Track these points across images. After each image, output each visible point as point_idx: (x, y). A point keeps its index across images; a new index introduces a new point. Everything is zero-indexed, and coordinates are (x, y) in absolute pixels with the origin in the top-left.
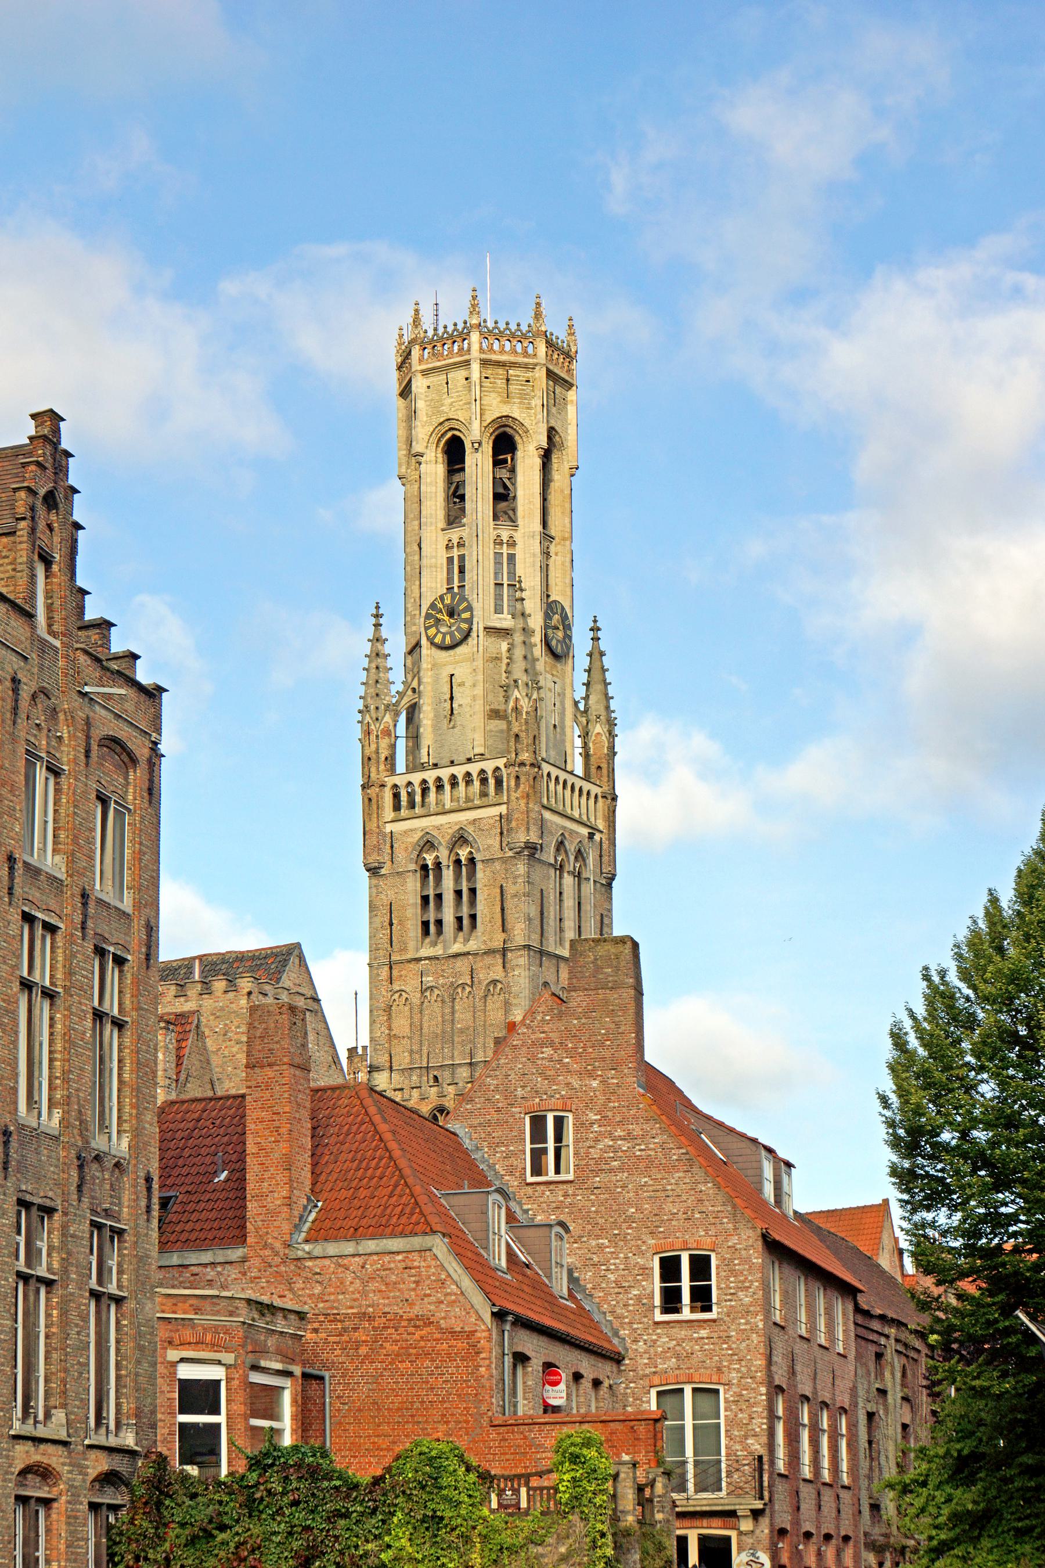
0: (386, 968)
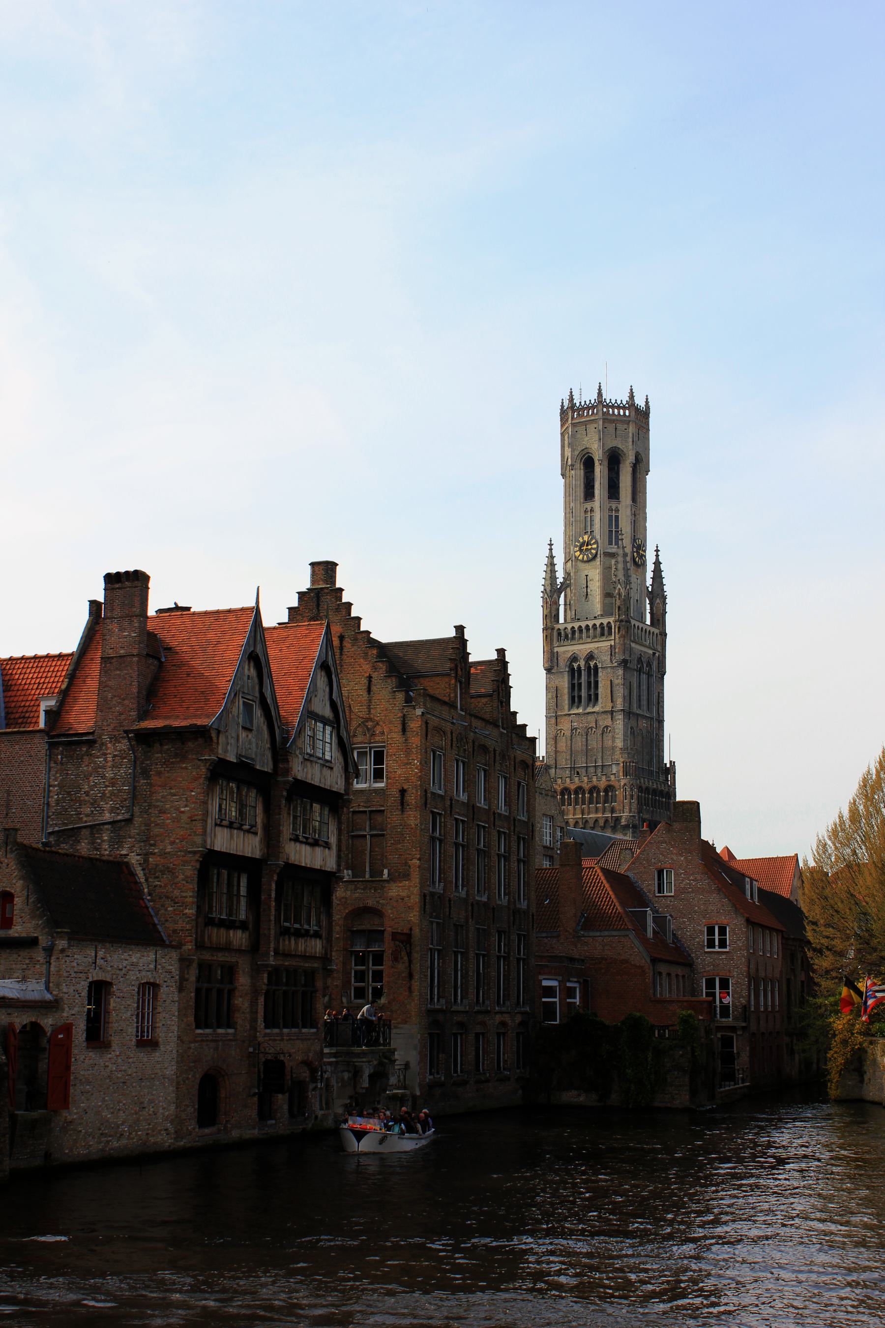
0: (554, 718)
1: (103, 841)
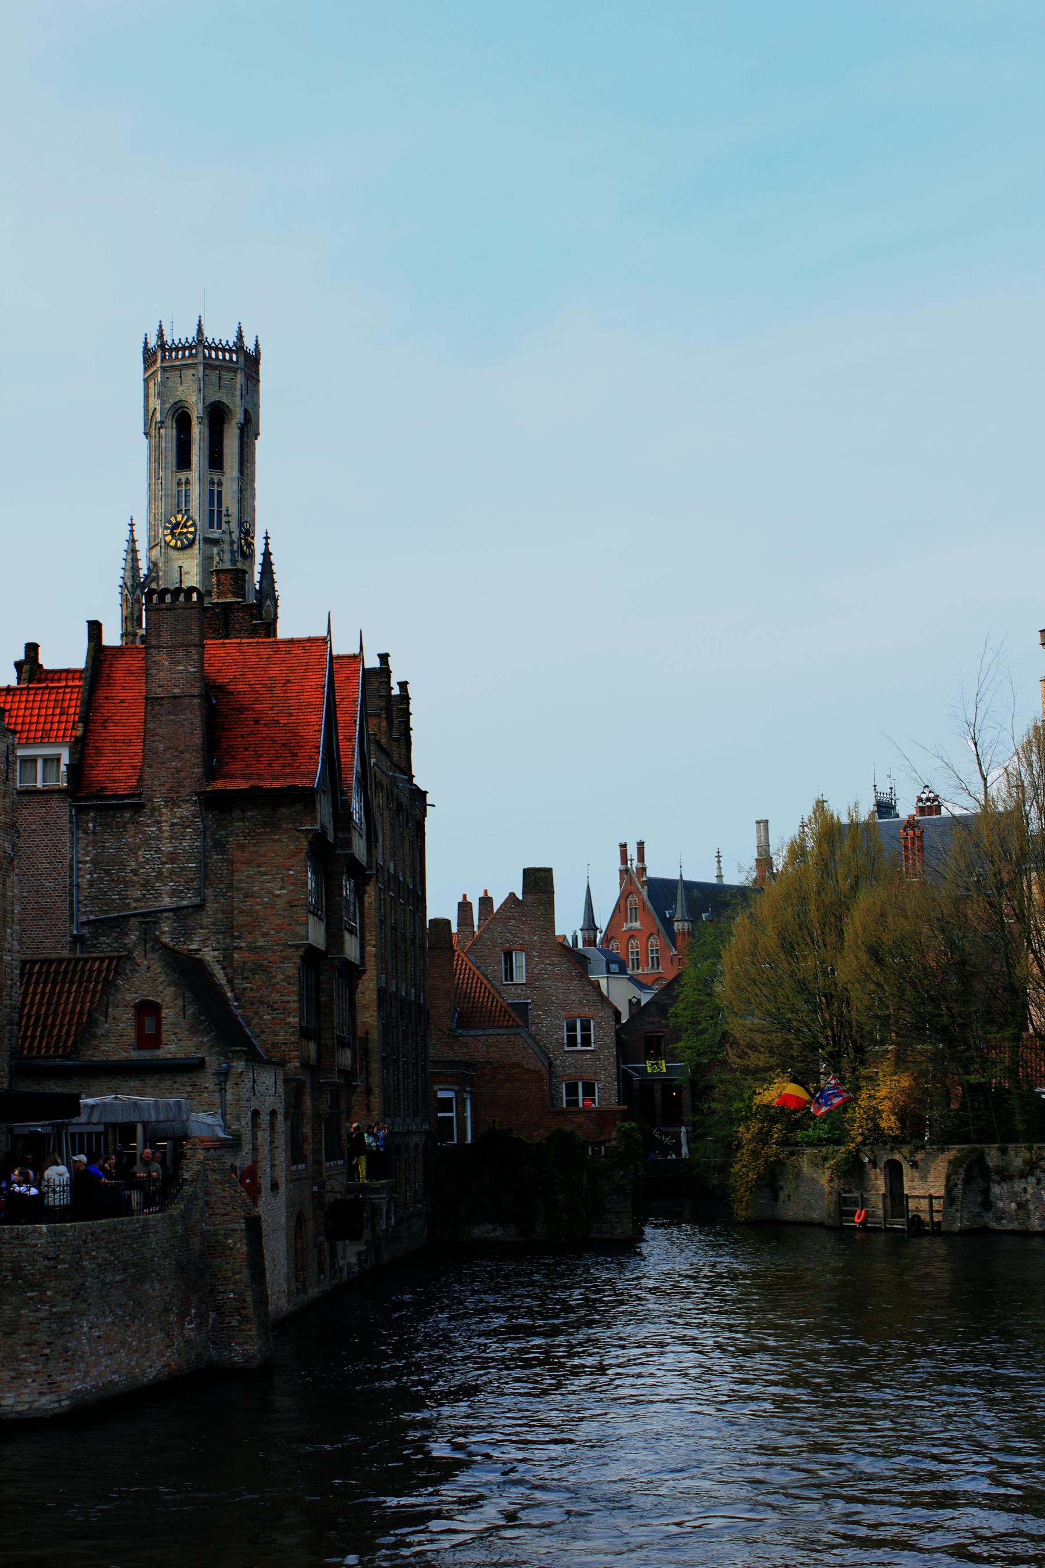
1: (164, 932)
